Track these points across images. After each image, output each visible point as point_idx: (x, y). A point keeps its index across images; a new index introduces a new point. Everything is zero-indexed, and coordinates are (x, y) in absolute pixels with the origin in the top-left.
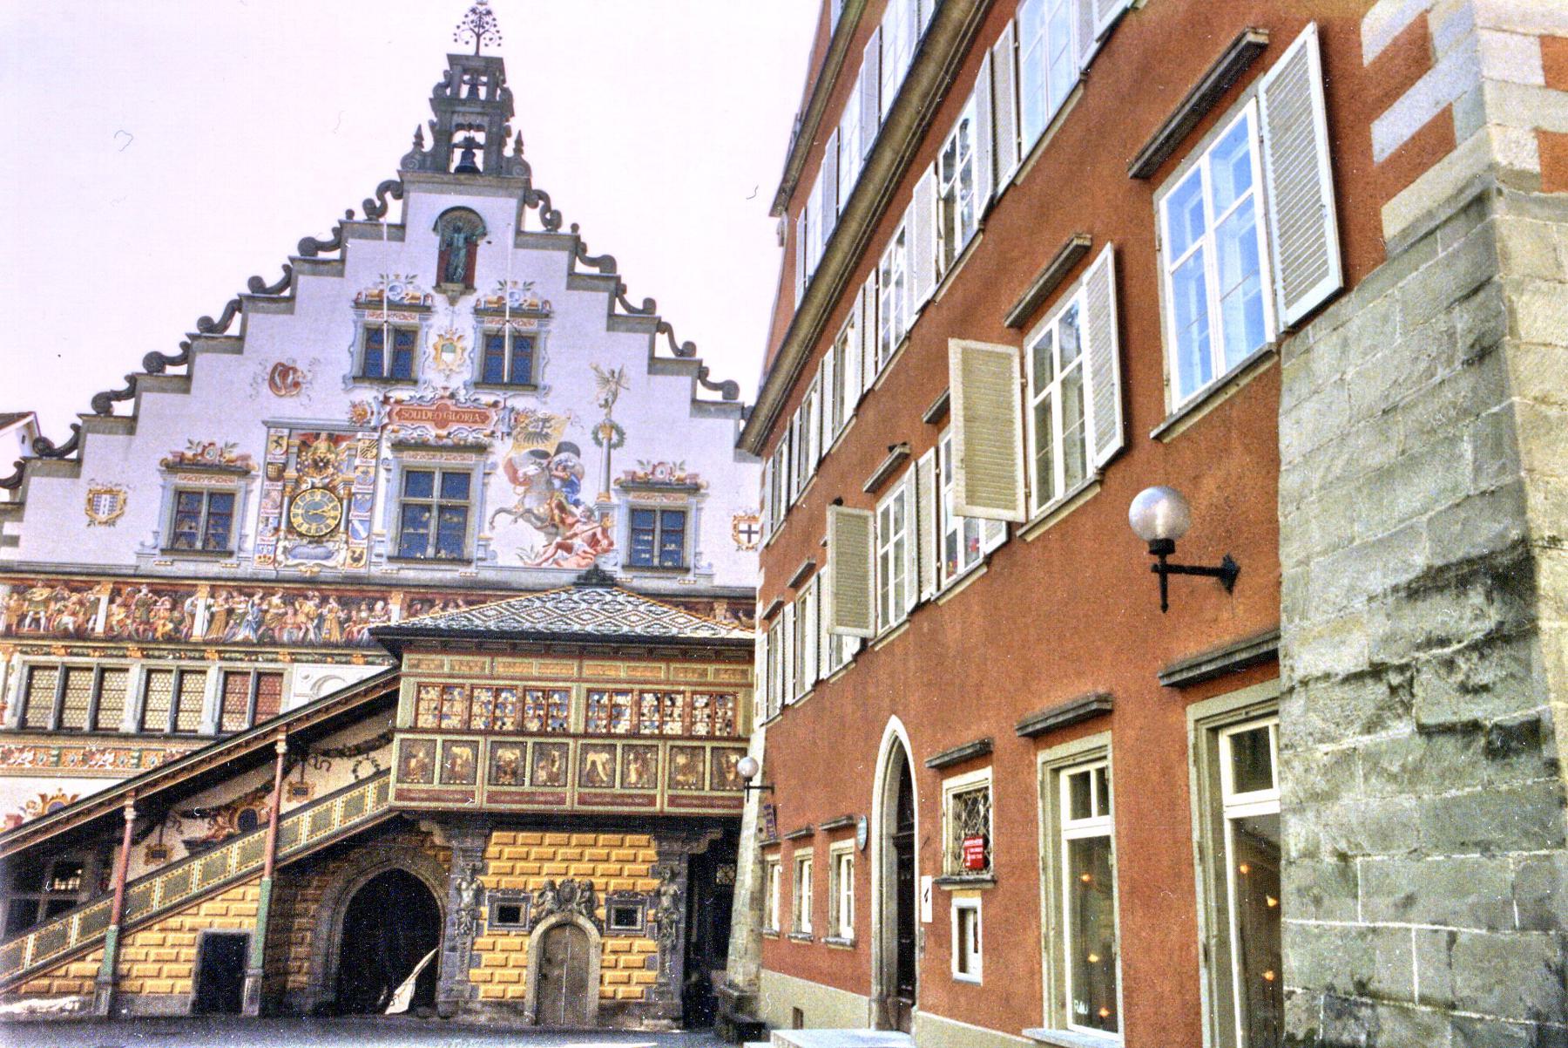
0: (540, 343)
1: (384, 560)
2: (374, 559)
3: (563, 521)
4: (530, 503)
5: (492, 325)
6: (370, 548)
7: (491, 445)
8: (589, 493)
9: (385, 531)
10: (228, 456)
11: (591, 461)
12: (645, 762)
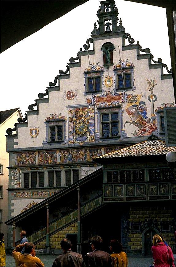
3: (143, 123)
5: (119, 73)
7: (122, 105)
8: (149, 114)
9: (98, 131)
11: (148, 106)
12: (165, 188)
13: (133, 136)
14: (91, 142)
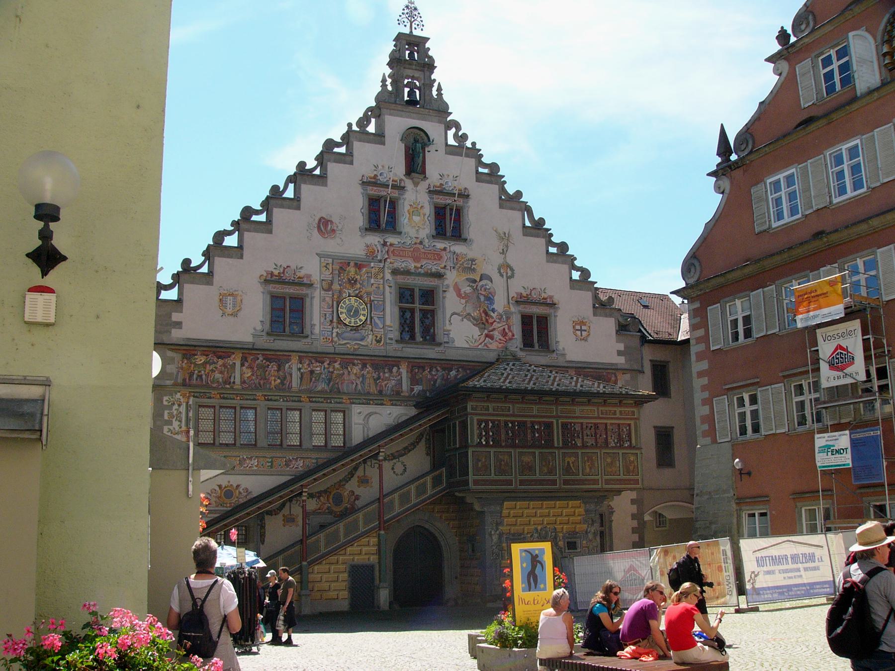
0: (465, 211)
1: (393, 342)
2: (388, 341)
3: (487, 321)
5: (441, 200)
6: (385, 335)
8: (500, 304)
10: (299, 274)
11: (498, 284)
13: (469, 347)
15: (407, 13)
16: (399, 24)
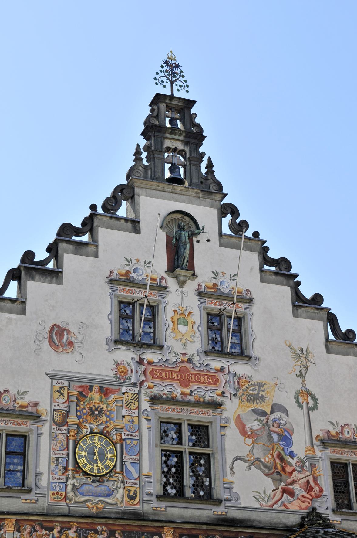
1: (153, 498)
2: (146, 498)
3: (283, 469)
4: (258, 453)
5: (215, 306)
6: (142, 487)
10: (20, 402)
13: (258, 506)
14: (127, 506)
15: (166, 71)
16: (156, 84)
